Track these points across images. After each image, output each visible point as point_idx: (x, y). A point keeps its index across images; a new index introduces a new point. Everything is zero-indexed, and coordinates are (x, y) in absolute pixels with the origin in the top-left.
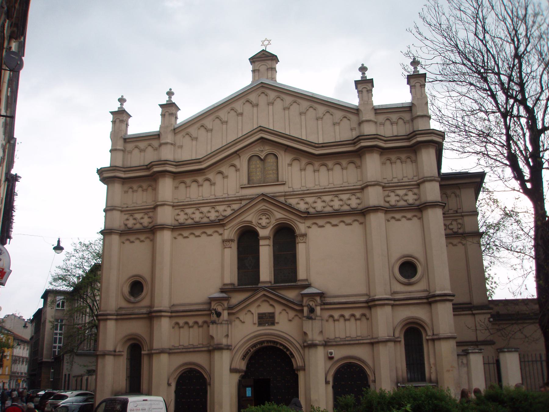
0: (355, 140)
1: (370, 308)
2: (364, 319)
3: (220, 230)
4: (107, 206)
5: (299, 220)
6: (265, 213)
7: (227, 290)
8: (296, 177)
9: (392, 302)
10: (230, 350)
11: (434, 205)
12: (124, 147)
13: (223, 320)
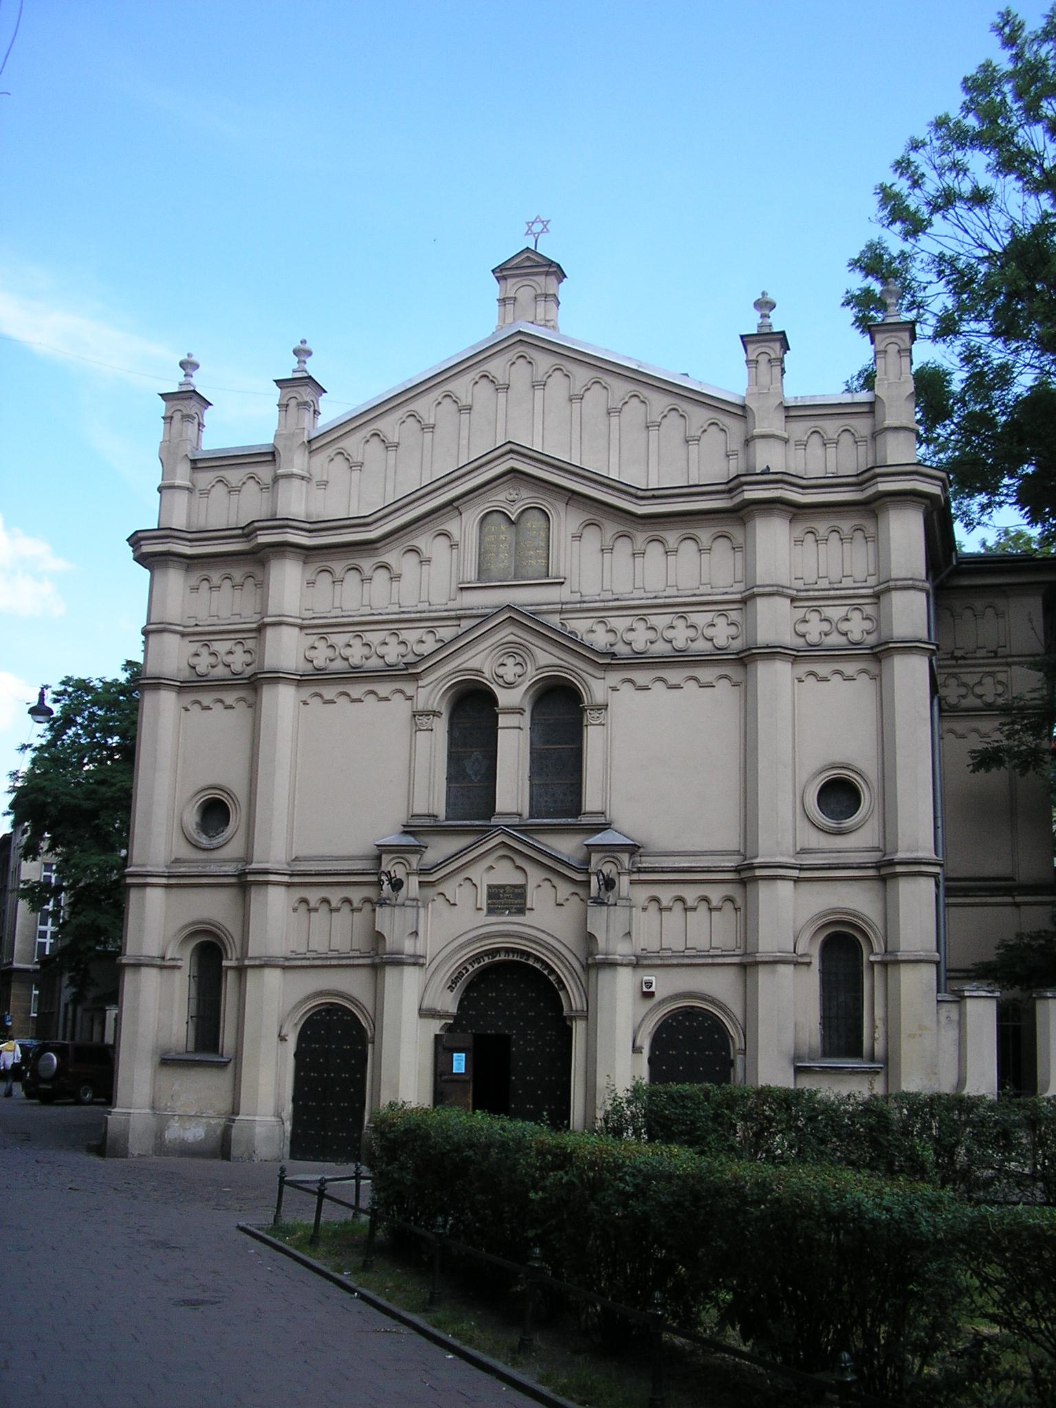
0: (731, 485)
1: (743, 882)
2: (729, 905)
3: (409, 688)
4: (149, 623)
5: (591, 670)
6: (514, 651)
7: (419, 829)
9: (795, 873)
10: (422, 965)
11: (909, 647)
12: (191, 481)
13: (408, 899)
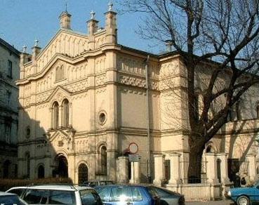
6: (59, 95)
8: (72, 74)
